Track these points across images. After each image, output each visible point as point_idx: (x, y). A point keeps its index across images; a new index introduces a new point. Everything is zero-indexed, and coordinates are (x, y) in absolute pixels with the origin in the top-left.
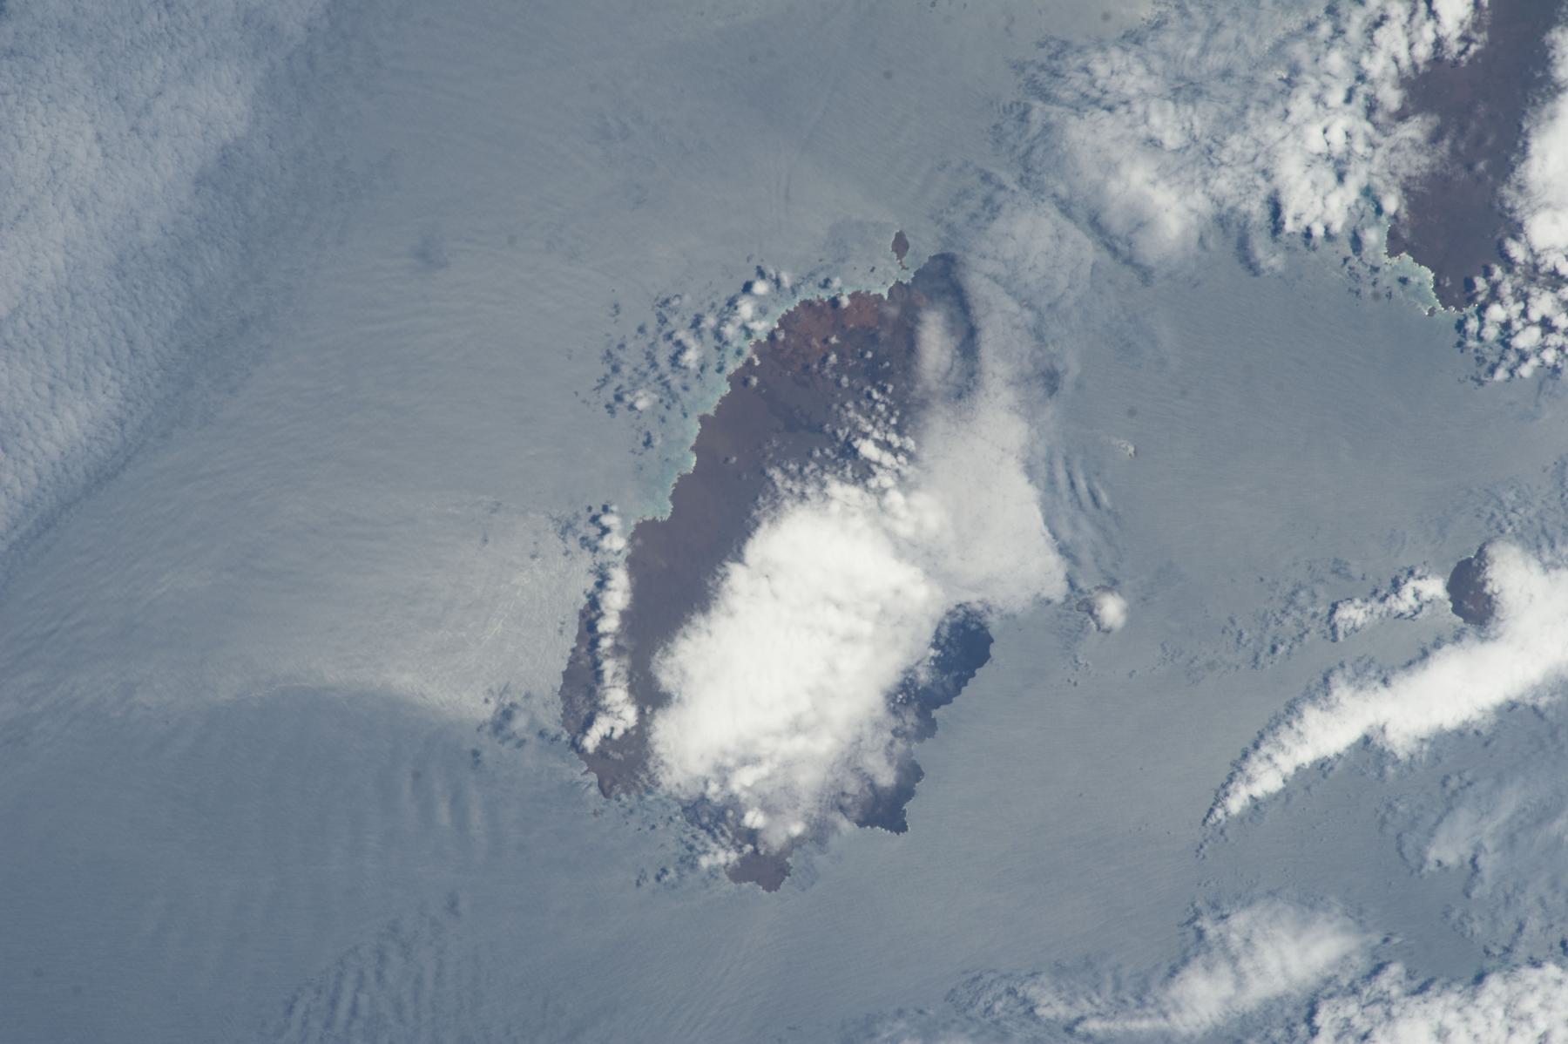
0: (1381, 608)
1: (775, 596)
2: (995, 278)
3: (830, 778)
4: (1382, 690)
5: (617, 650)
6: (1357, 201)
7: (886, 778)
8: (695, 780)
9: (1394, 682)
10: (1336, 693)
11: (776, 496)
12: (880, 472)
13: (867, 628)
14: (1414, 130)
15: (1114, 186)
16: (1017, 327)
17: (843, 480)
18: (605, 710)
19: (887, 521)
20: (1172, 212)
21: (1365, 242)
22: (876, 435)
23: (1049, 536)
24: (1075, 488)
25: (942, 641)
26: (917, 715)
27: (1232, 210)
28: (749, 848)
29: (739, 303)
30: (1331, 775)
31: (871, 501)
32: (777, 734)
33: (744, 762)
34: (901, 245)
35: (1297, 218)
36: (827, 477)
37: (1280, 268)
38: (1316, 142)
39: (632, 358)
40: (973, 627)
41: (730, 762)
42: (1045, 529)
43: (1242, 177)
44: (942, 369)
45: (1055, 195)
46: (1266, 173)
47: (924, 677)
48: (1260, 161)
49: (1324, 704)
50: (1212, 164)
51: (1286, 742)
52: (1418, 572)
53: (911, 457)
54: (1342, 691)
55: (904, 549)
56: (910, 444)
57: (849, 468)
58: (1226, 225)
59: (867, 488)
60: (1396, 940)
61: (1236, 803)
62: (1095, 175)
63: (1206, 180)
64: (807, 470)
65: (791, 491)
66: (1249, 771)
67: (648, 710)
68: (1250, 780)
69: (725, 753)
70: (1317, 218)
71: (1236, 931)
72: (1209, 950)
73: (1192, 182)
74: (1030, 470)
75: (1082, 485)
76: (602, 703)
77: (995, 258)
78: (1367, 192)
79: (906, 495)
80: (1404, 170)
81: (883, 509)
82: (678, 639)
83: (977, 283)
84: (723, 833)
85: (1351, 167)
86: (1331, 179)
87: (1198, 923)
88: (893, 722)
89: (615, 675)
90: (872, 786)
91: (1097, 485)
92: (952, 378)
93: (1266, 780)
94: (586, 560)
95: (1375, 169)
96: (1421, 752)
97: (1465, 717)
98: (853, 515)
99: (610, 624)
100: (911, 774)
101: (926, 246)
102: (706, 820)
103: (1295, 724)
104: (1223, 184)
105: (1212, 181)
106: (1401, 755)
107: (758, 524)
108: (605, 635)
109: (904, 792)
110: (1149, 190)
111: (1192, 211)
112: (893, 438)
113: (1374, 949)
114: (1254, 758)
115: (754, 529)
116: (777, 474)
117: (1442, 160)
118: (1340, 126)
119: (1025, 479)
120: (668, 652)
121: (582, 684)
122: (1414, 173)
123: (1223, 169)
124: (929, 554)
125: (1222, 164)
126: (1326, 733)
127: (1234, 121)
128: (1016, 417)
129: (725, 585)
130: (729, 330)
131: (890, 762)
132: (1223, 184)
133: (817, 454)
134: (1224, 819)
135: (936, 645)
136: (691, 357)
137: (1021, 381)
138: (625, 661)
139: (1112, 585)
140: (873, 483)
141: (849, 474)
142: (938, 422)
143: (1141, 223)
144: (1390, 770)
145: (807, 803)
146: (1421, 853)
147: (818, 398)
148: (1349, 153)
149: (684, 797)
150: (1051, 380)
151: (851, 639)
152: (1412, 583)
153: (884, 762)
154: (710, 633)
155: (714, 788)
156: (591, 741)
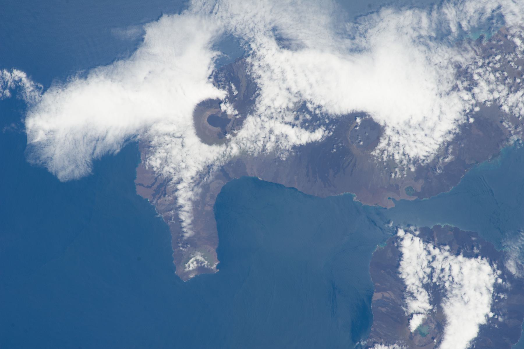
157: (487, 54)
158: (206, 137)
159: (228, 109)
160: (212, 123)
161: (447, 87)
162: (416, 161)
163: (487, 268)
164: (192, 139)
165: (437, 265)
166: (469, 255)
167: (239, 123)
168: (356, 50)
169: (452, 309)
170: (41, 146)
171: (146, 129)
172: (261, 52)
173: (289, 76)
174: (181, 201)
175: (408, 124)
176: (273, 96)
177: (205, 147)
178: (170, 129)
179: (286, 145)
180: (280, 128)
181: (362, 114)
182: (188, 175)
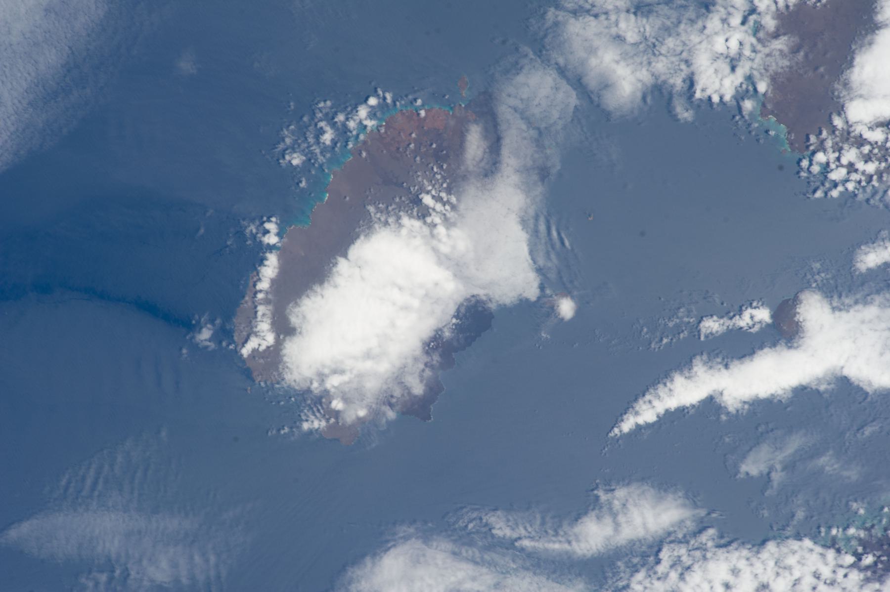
0: (730, 323)
1: (363, 279)
2: (516, 110)
3: (385, 387)
4: (724, 371)
5: (267, 302)
6: (741, 84)
8: (305, 380)
9: (731, 367)
10: (695, 369)
11: (370, 220)
12: (433, 214)
13: (416, 303)
15: (593, 62)
16: (525, 138)
17: (411, 216)
18: (256, 334)
19: (435, 242)
20: (625, 81)
21: (744, 109)
22: (433, 192)
23: (530, 261)
25: (461, 315)
26: (440, 356)
27: (665, 82)
28: (332, 420)
29: (359, 108)
30: (687, 416)
31: (426, 230)
32: (355, 358)
33: (335, 372)
35: (703, 90)
36: (402, 213)
37: (690, 119)
40: (480, 309)
41: (326, 371)
42: (529, 258)
43: (672, 63)
44: (477, 159)
45: (557, 64)
46: (687, 63)
47: (447, 334)
48: (685, 55)
49: (687, 375)
50: (654, 54)
51: (661, 394)
52: (755, 304)
53: (454, 208)
54: (699, 368)
55: (443, 260)
56: (453, 199)
57: (416, 209)
59: (425, 223)
60: (714, 515)
61: (627, 425)
62: (582, 54)
63: (650, 63)
64: (390, 208)
65: (379, 219)
66: (637, 408)
67: (281, 337)
68: (637, 413)
69: (324, 366)
70: (716, 91)
71: (618, 499)
72: (601, 507)
73: (641, 63)
74: (523, 222)
75: (554, 233)
76: (255, 330)
77: (516, 97)
78: (749, 78)
79: (448, 228)
80: (773, 67)
81: (432, 236)
82: (304, 297)
83: (504, 111)
84: (318, 410)
85: (741, 63)
86: (727, 69)
87: (596, 492)
88: (426, 359)
89: (264, 315)
90: (409, 393)
91: (563, 235)
92: (482, 164)
93: (647, 413)
95: (755, 66)
96: (743, 409)
97: (773, 392)
98: (415, 237)
102: (309, 402)
103: (668, 384)
104: (661, 66)
105: (654, 64)
106: (731, 409)
107: (358, 237)
108: (261, 291)
110: (614, 66)
111: (640, 81)
112: (443, 195)
113: (702, 518)
114: (641, 402)
115: (356, 239)
116: (371, 209)
117: (797, 63)
119: (520, 227)
120: (297, 305)
122: (780, 70)
123: (661, 58)
124: (457, 265)
125: (661, 54)
126: (685, 391)
128: (519, 191)
129: (334, 270)
130: (352, 124)
131: (421, 381)
132: (661, 66)
133: (397, 200)
134: (619, 434)
135: (456, 316)
136: (328, 137)
137: (524, 170)
138: (270, 307)
140: (429, 220)
141: (415, 214)
142: (471, 190)
143: (606, 85)
144: (724, 417)
145: (370, 399)
146: (736, 467)
148: (740, 54)
149: (297, 388)
150: (543, 173)
151: (406, 308)
152: (749, 311)
153: (418, 381)
154: (323, 296)
155: (315, 385)
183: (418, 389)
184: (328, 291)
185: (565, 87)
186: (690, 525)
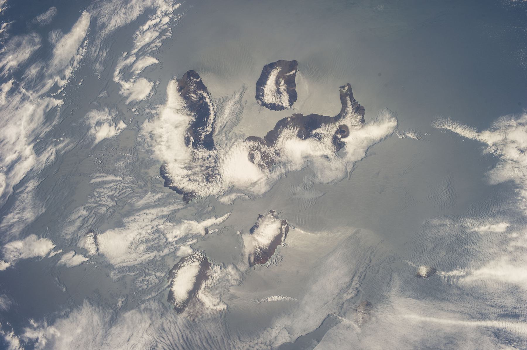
7: (260, 219)
14: (208, 274)
24: (240, 244)
34: (255, 269)
38: (217, 274)
39: (280, 260)
54: (219, 223)
55: (257, 240)
58: (225, 268)
61: (229, 214)
83: (248, 264)
93: (226, 216)
94: (286, 242)
99: (284, 236)
100: (258, 220)
101: (252, 268)
104: (225, 271)
109: (259, 218)
118: (215, 275)
121: (287, 231)
126: (220, 219)
127: (224, 277)
132: (225, 271)
139: (238, 235)
142: (253, 252)
143: (233, 268)
147: (263, 255)
150: (242, 255)
156: (286, 225)
157: (273, 161)
158: (345, 126)
159: (339, 136)
160: (344, 131)
161: (282, 150)
162: (287, 128)
163: (266, 101)
164: (349, 125)
165: (279, 100)
166: (271, 104)
167: (337, 132)
168: (306, 157)
169: (274, 88)
170: (392, 117)
171: (362, 126)
172: (332, 153)
173: (324, 148)
174: (351, 107)
175: (291, 139)
176: (328, 141)
177: (345, 124)
178: (356, 128)
179: (323, 127)
180: (325, 132)
181: (303, 139)
182: (349, 115)
183: (260, 219)
184: (274, 235)
185: (239, 268)
186: (219, 198)
